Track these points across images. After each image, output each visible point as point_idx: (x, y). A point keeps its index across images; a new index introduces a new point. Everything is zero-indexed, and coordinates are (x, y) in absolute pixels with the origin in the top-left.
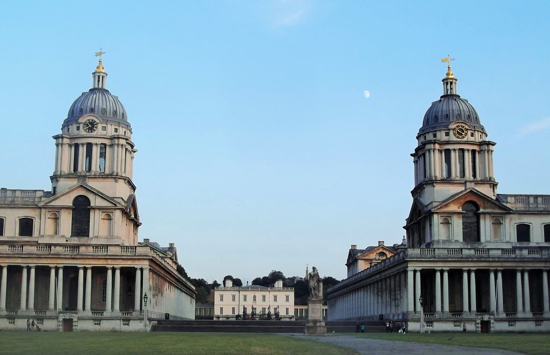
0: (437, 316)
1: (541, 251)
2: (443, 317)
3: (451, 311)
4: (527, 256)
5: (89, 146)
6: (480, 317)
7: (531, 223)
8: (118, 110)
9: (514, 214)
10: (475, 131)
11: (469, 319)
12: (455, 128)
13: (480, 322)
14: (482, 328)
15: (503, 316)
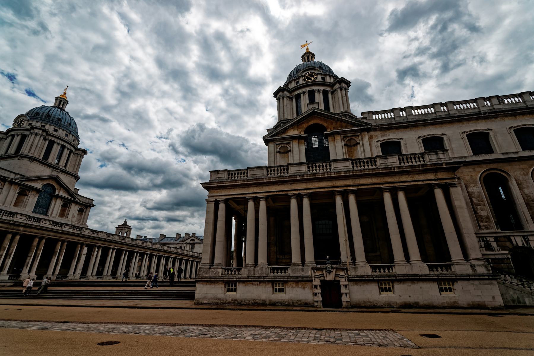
0: (244, 273)
1: (423, 158)
2: (254, 274)
3: (269, 263)
4: (400, 166)
5: (13, 136)
6: (318, 274)
7: (400, 139)
8: (52, 116)
9: (375, 130)
10: (326, 75)
11: (297, 277)
12: (304, 75)
13: (320, 283)
14: (322, 294)
15: (366, 270)
